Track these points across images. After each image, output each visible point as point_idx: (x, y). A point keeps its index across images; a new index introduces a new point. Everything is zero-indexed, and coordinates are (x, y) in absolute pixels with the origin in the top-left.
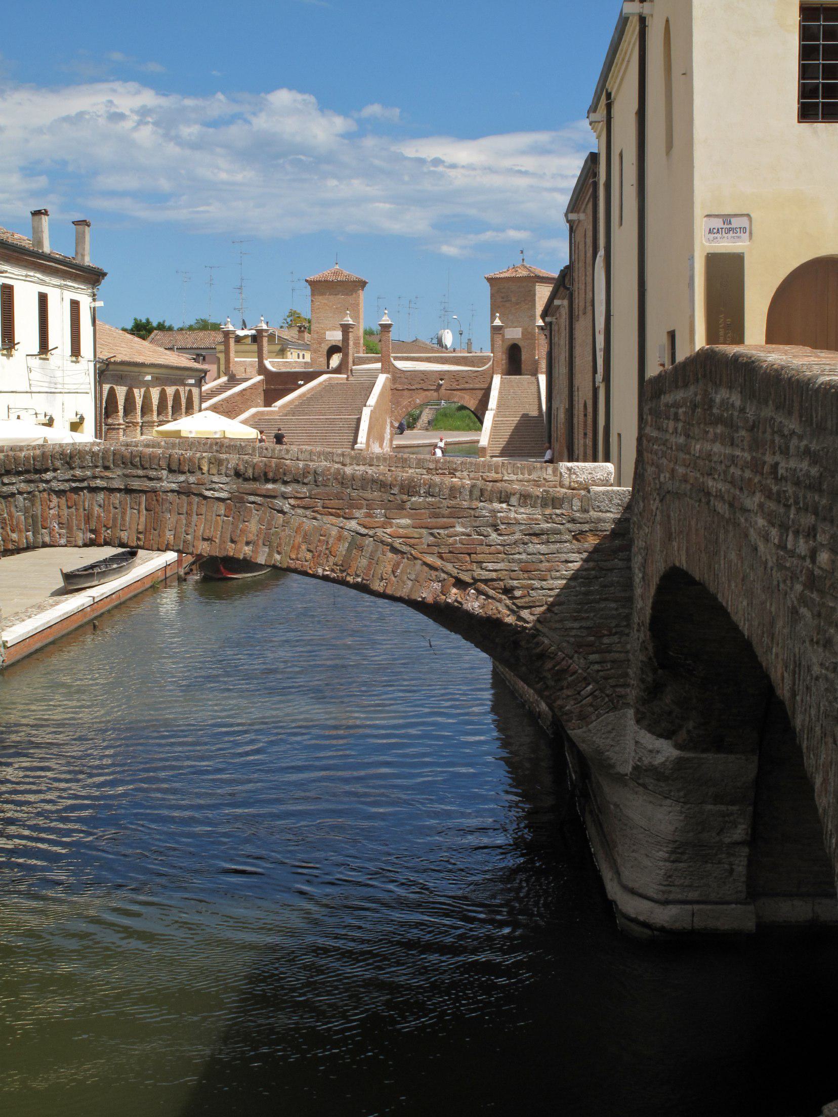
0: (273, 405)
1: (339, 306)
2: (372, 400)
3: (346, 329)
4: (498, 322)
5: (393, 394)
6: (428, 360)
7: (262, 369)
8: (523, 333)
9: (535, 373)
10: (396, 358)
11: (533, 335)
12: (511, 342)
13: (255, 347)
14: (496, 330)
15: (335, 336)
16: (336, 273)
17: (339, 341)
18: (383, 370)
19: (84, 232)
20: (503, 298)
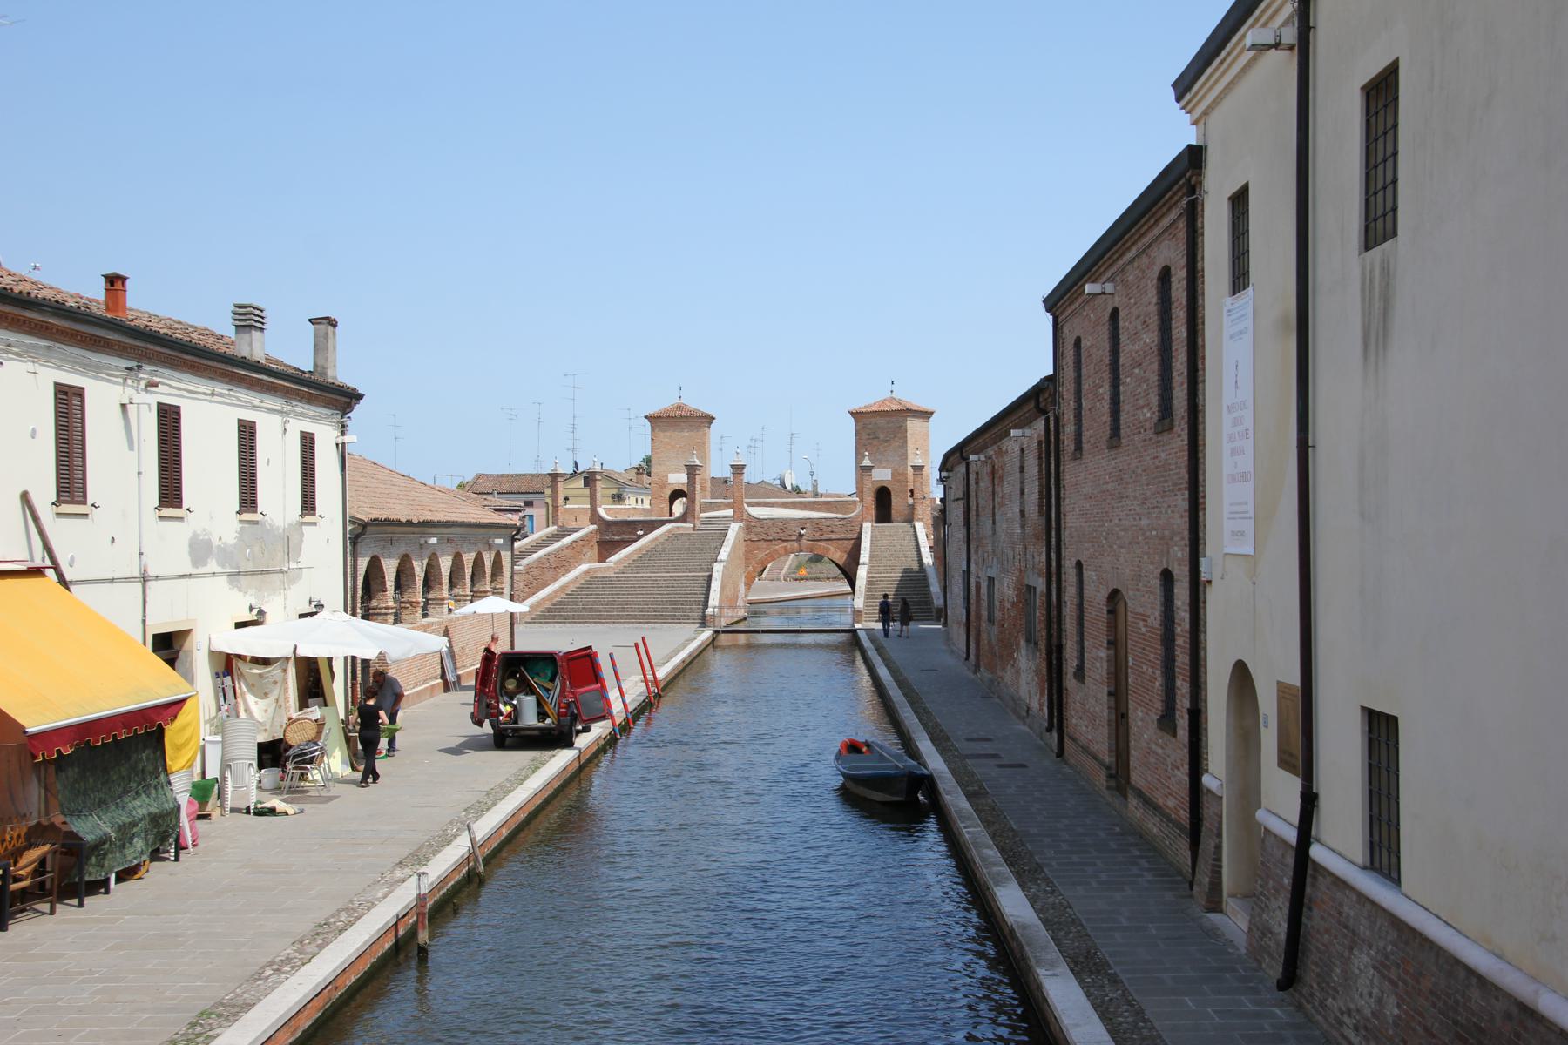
0: (607, 560)
1: (682, 445)
2: (724, 554)
3: (692, 470)
4: (867, 462)
5: (747, 546)
6: (785, 505)
7: (595, 517)
8: (893, 474)
9: (910, 520)
10: (750, 504)
11: (904, 474)
12: (879, 485)
13: (587, 491)
14: (863, 471)
15: (679, 479)
16: (679, 407)
17: (683, 484)
18: (734, 519)
19: (327, 334)
20: (869, 435)
